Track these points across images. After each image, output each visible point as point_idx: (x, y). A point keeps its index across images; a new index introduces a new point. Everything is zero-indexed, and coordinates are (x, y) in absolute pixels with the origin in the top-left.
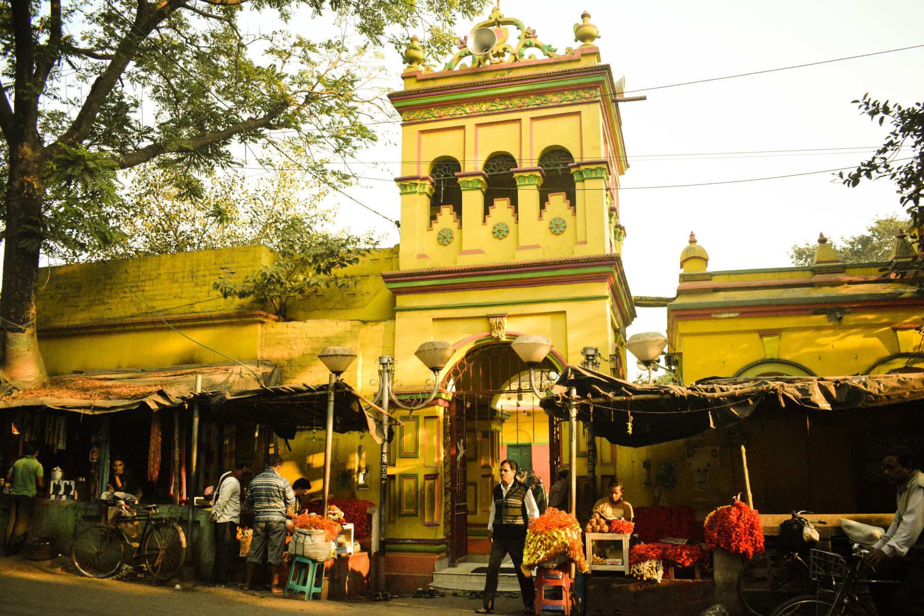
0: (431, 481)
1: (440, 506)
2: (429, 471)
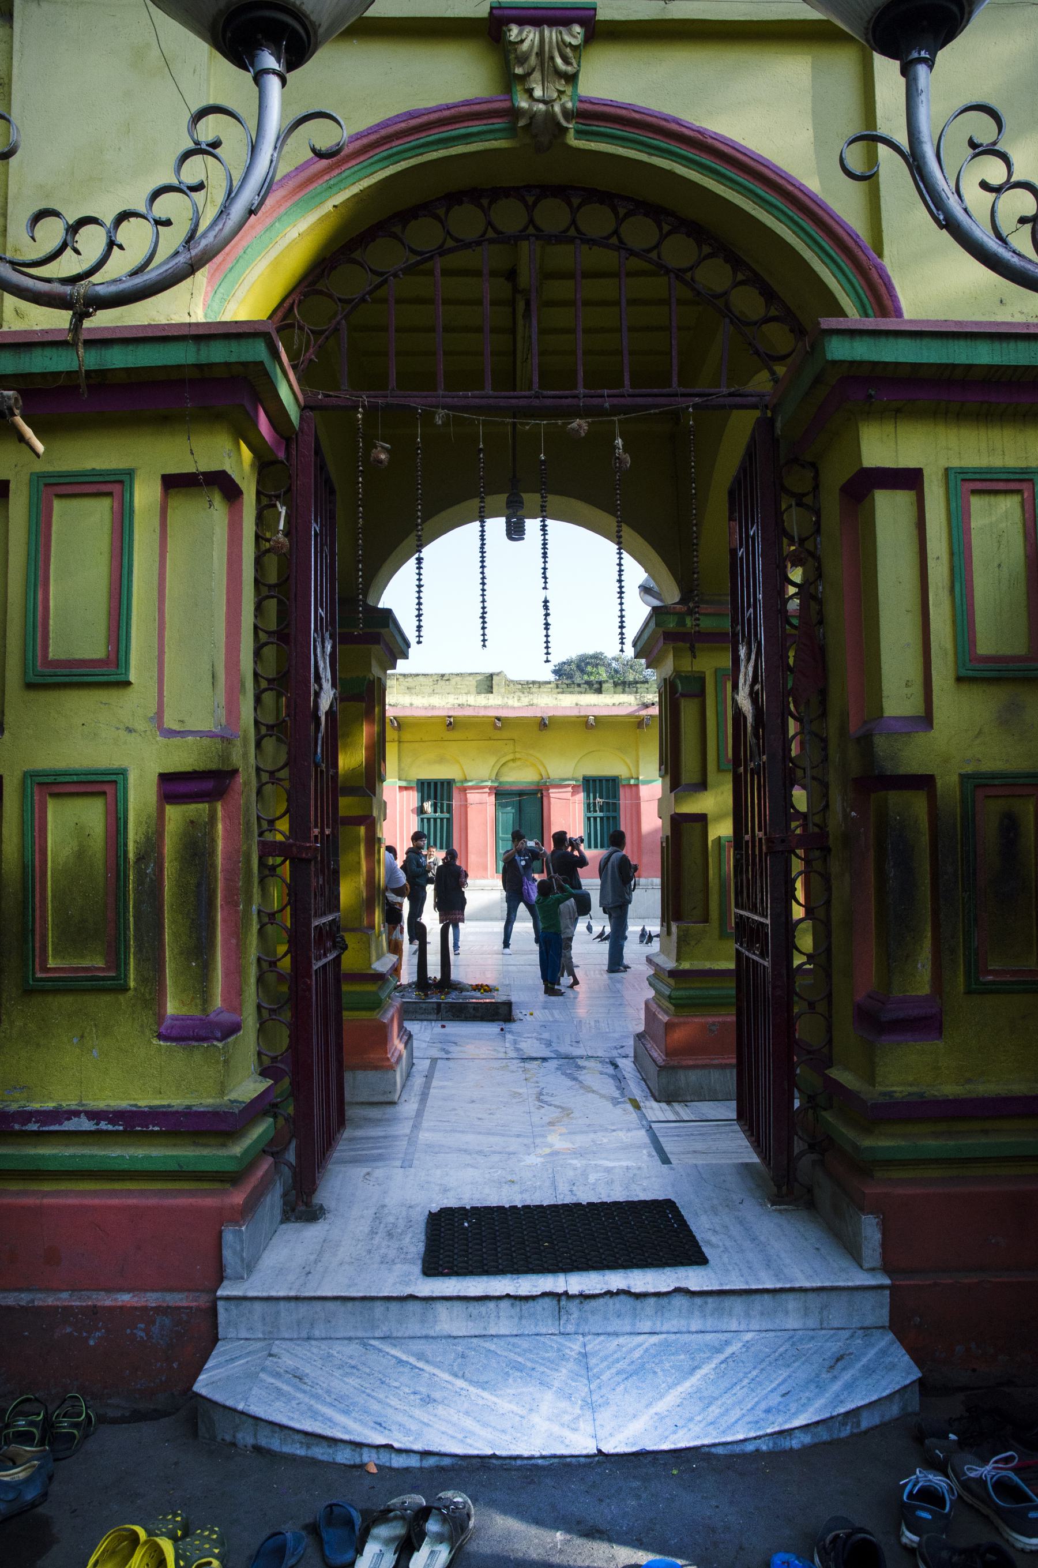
0: (203, 807)
1: (237, 932)
2: (183, 758)
